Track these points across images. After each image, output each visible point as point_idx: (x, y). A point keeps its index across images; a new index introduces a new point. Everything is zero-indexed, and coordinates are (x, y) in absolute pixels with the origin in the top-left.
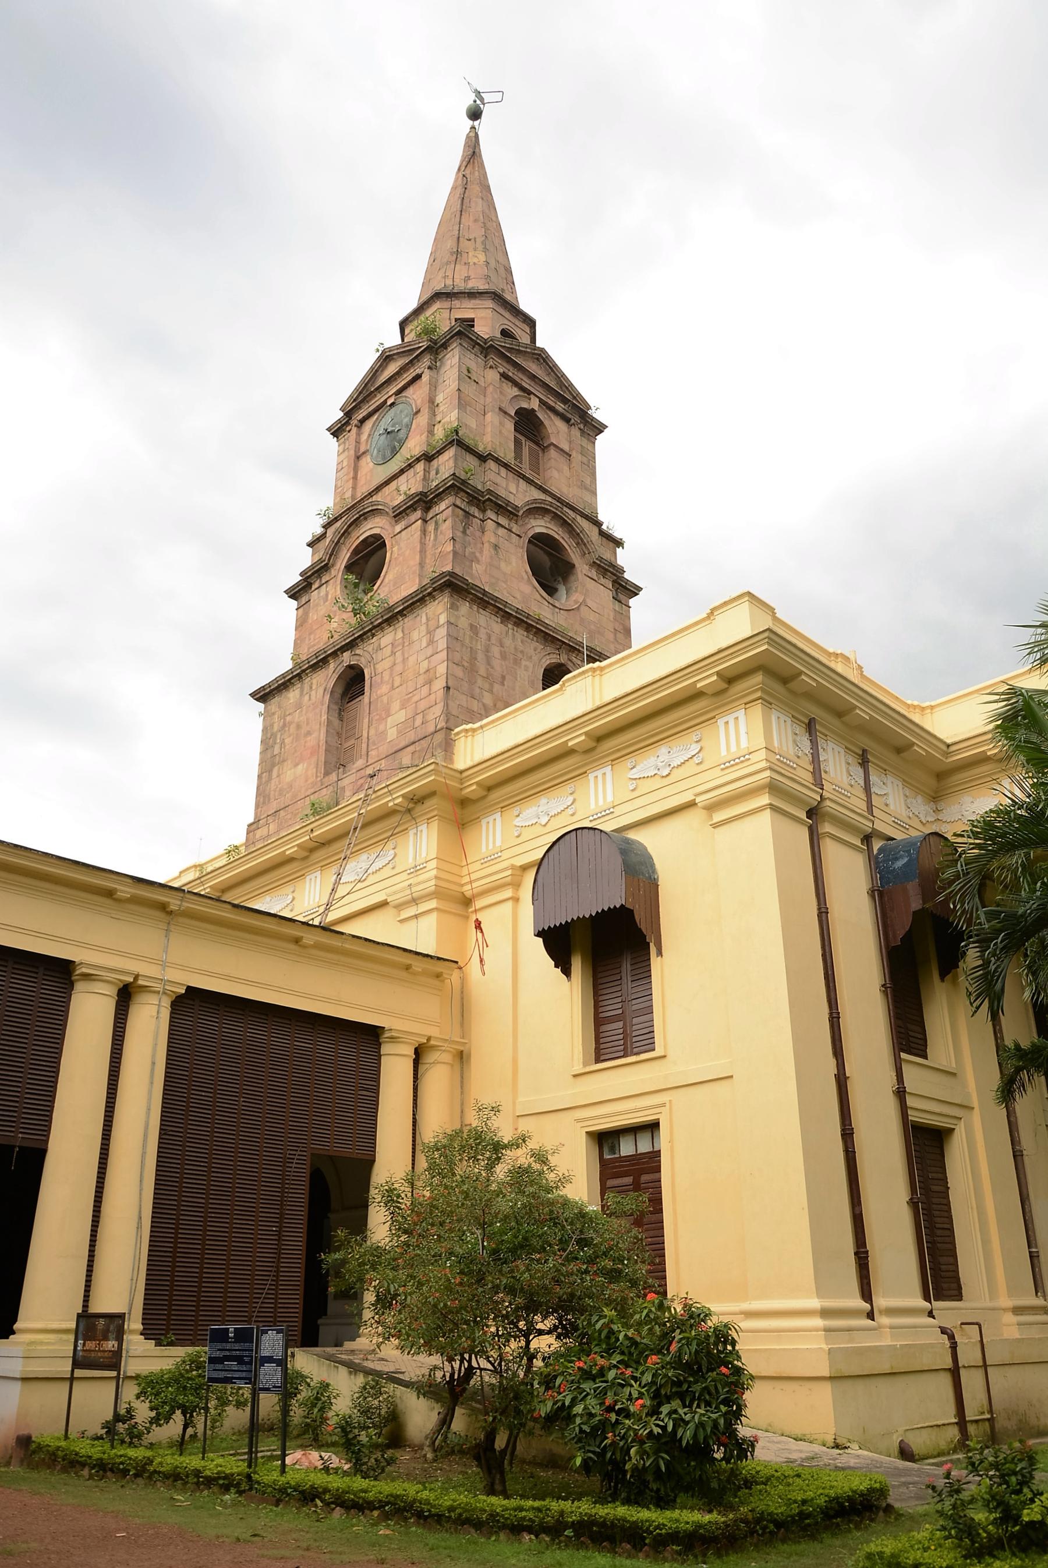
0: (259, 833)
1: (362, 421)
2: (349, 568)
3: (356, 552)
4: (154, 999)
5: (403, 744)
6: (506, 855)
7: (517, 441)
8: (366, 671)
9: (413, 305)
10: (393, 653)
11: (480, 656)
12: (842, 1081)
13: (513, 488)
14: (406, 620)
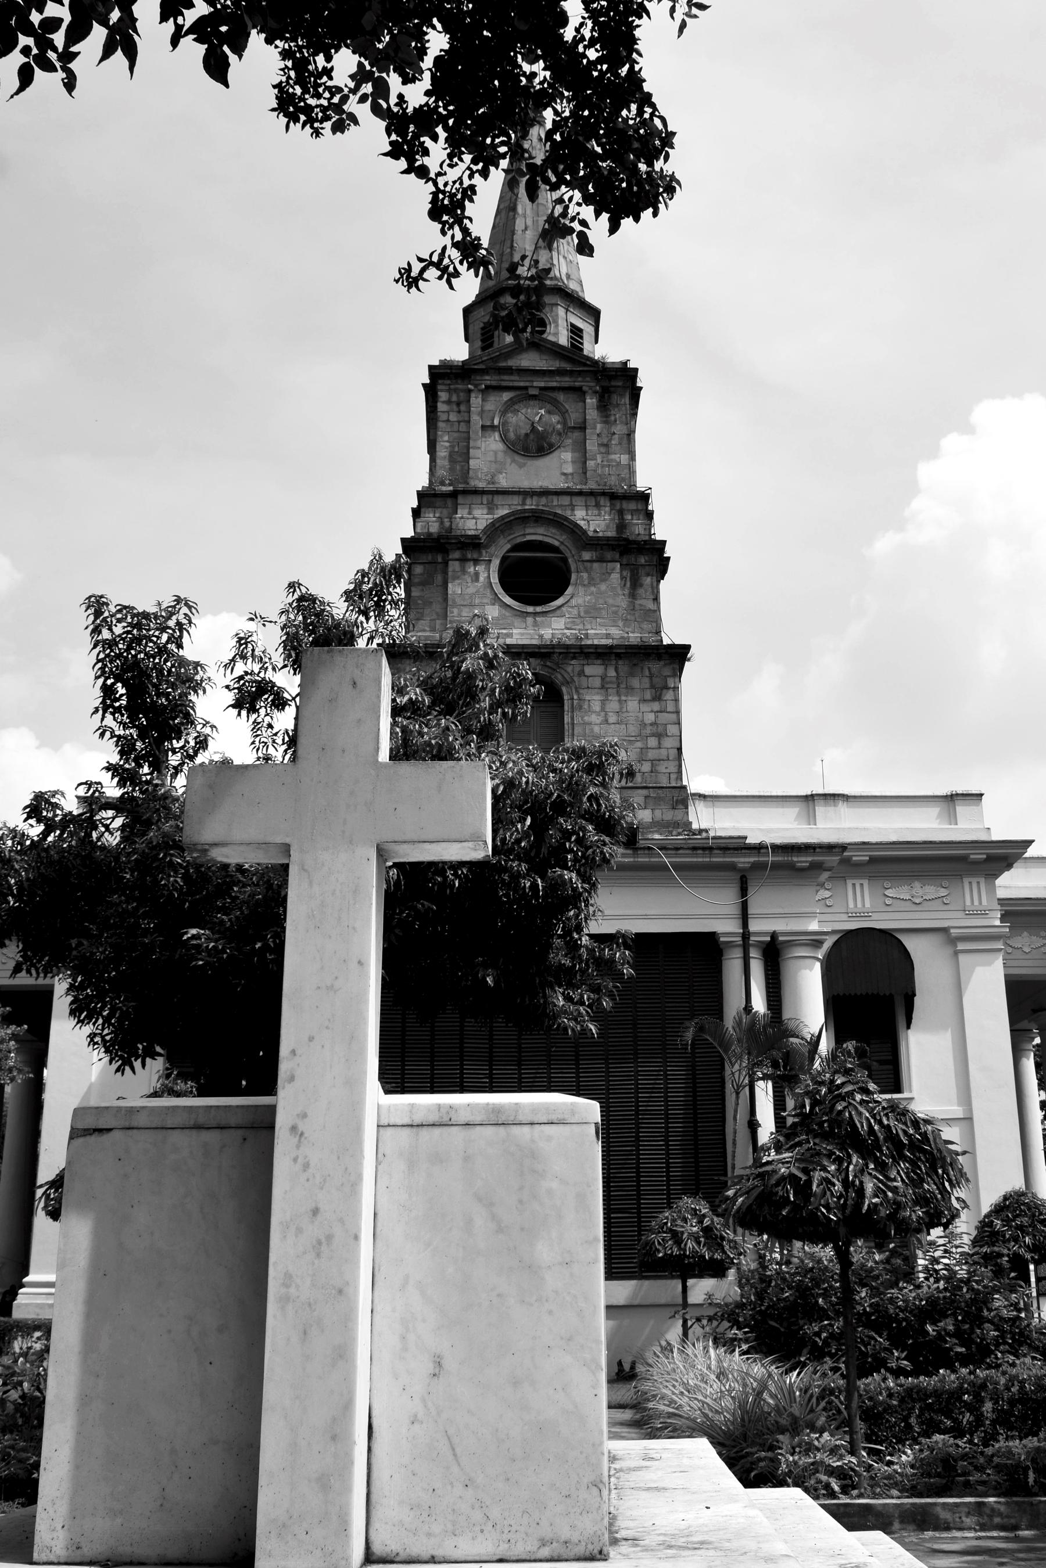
3: (516, 548)
14: (620, 662)
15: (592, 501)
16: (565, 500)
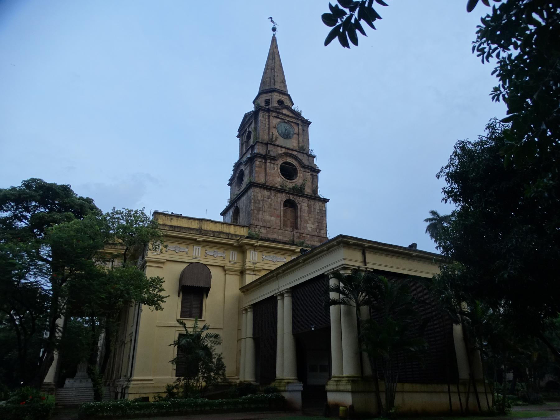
8: (298, 205)
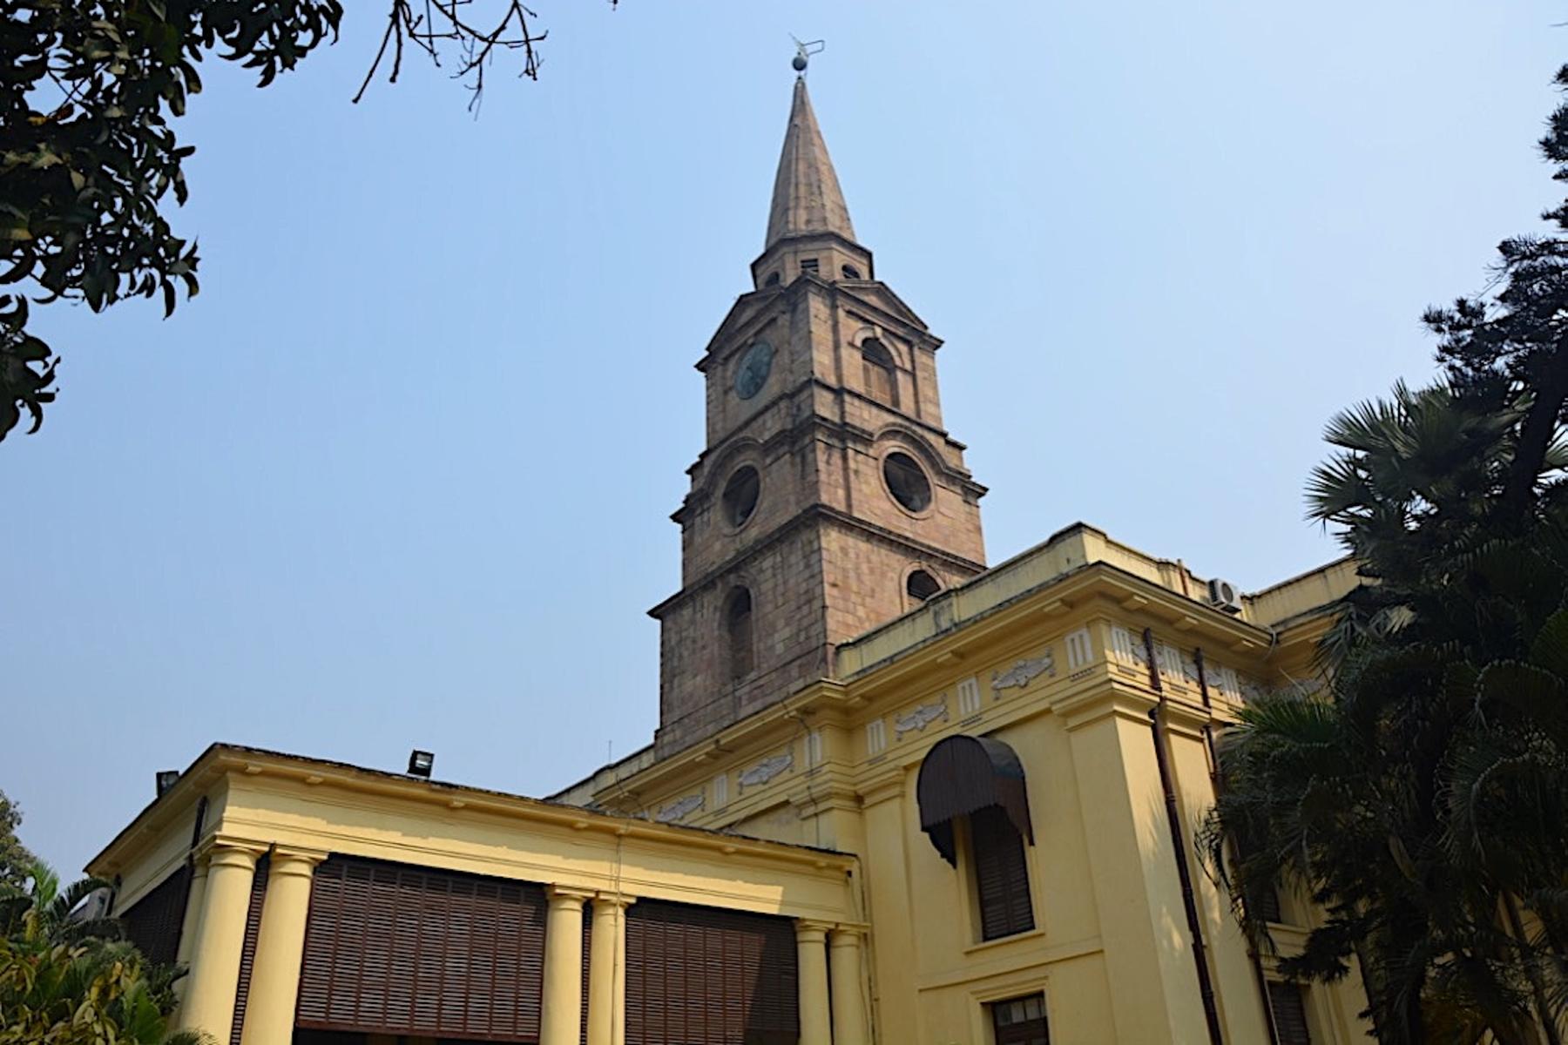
0: (667, 739)
1: (726, 359)
2: (725, 495)
3: (732, 481)
4: (611, 911)
5: (789, 658)
6: (890, 756)
7: (866, 369)
8: (752, 592)
9: (761, 250)
10: (774, 575)
11: (852, 574)
12: (1199, 950)
13: (866, 415)
15: (775, 410)
16: (760, 421)
